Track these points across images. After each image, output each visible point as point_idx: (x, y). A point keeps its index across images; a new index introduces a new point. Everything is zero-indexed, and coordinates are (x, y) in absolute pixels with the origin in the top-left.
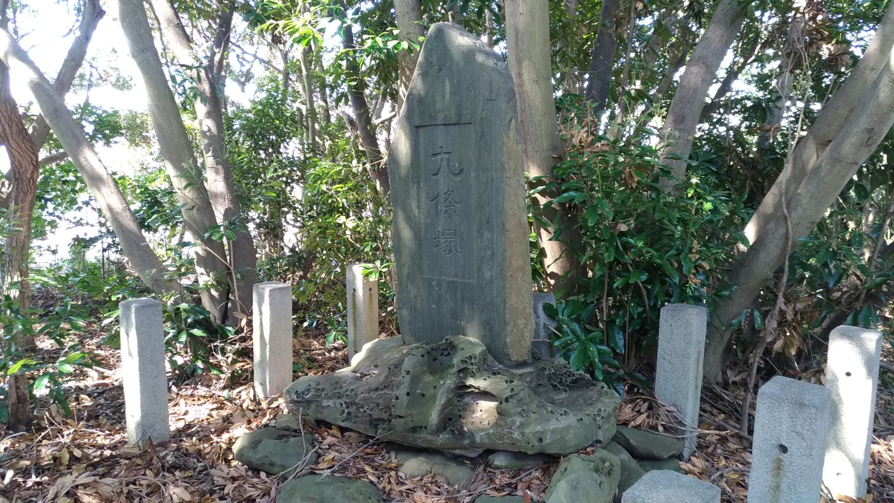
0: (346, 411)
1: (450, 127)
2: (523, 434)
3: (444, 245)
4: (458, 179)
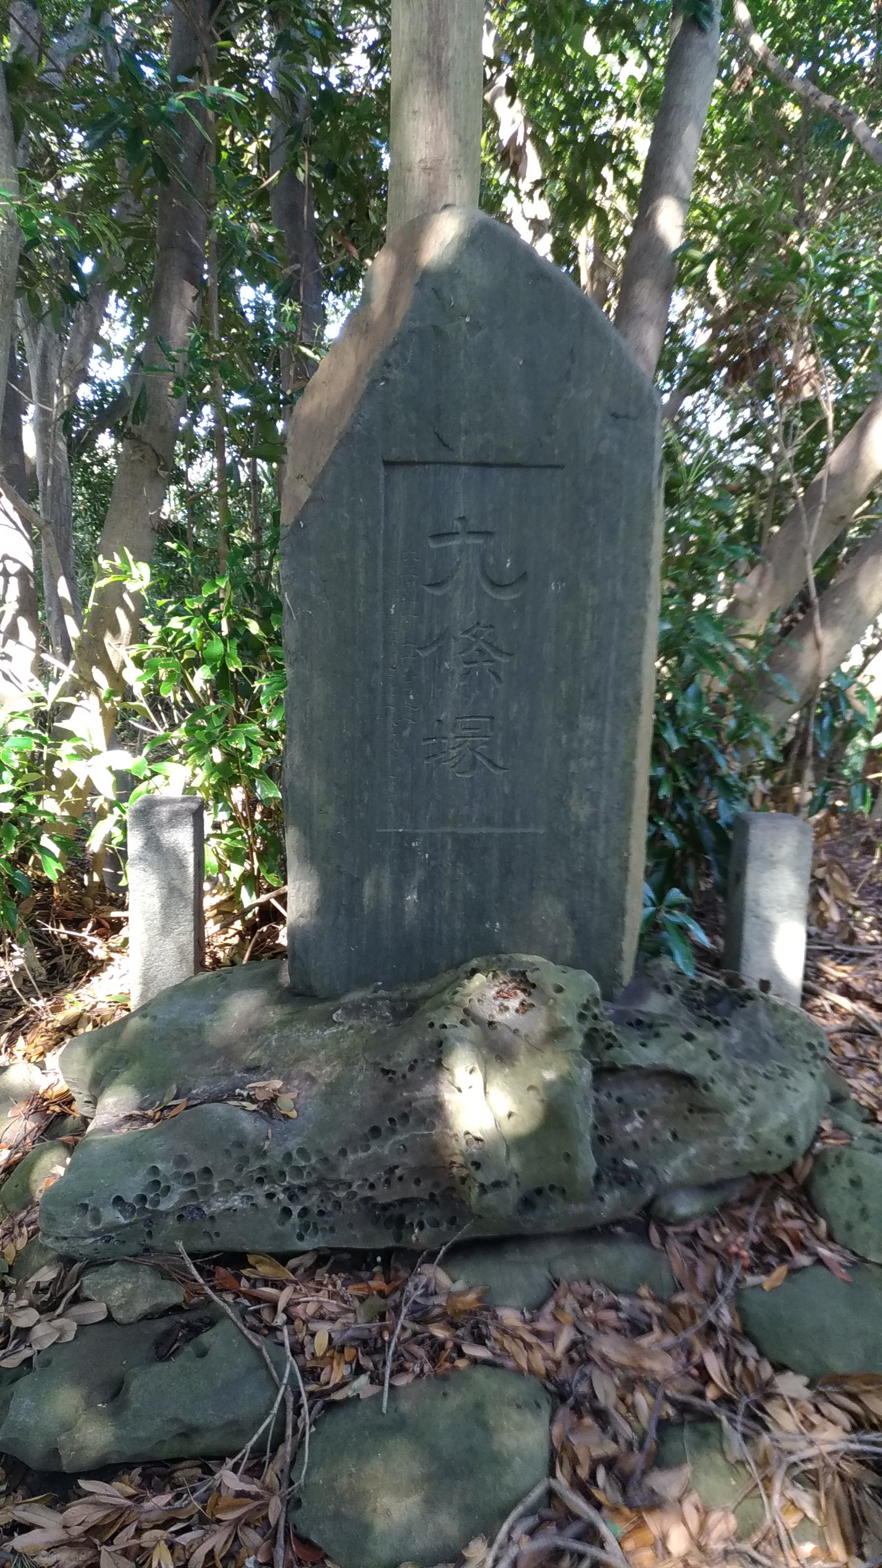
0: (296, 1209)
1: (494, 472)
2: (754, 1139)
3: (454, 753)
4: (507, 597)
